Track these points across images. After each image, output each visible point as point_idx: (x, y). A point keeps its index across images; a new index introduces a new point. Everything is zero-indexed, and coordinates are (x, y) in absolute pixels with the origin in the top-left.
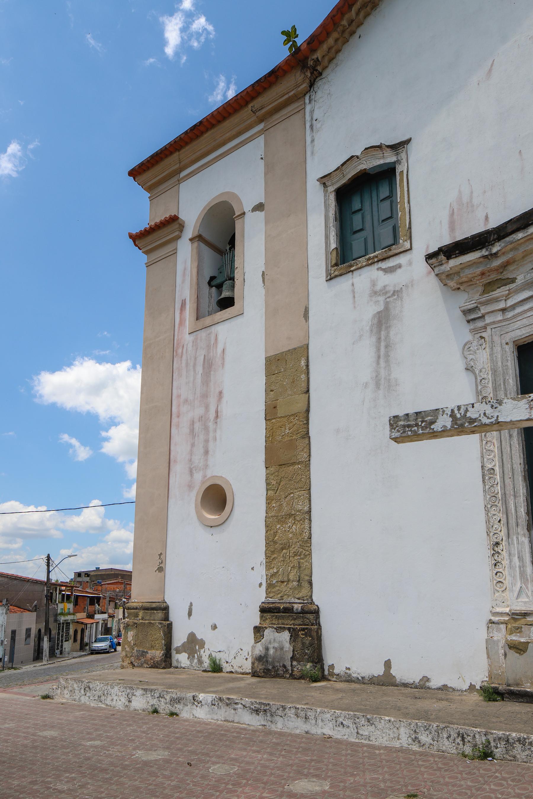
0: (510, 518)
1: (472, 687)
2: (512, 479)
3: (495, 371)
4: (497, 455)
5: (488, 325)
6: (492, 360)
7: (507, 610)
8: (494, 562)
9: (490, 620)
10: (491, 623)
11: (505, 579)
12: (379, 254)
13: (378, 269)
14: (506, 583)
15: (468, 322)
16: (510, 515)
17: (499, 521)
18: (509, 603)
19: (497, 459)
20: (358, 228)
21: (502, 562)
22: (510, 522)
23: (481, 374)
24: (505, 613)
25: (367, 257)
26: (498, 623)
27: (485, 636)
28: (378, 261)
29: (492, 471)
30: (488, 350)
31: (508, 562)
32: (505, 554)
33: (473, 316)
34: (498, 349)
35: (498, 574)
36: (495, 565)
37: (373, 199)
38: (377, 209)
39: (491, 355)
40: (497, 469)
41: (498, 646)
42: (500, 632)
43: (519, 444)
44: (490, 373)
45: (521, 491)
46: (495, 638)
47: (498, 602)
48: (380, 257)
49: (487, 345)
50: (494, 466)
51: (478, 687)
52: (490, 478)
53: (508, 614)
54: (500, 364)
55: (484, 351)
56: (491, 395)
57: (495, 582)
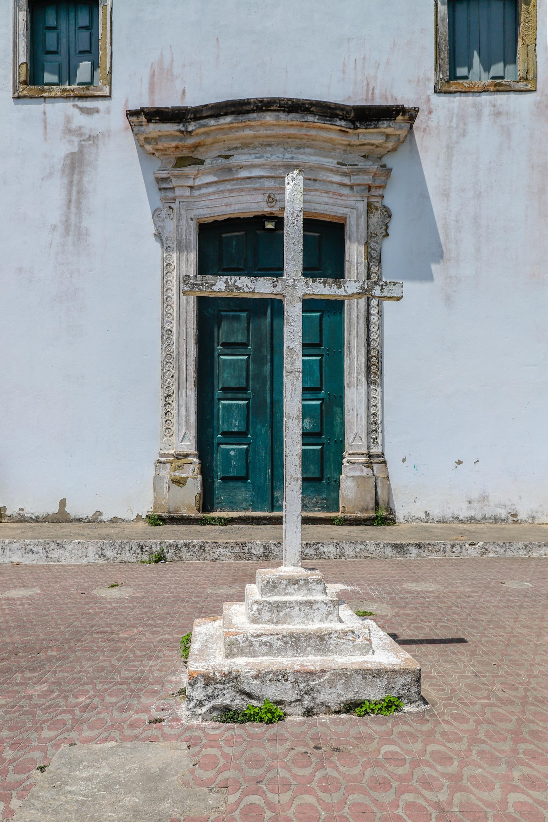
0: (181, 374)
1: (139, 518)
2: (185, 341)
3: (180, 242)
4: (175, 318)
5: (177, 197)
6: (178, 231)
7: (172, 452)
8: (165, 411)
9: (158, 460)
11: (173, 426)
12: (76, 89)
13: (74, 106)
14: (174, 429)
15: (160, 189)
16: (181, 371)
17: (172, 377)
18: (174, 446)
19: (174, 322)
20: (52, 49)
21: (172, 412)
22: (181, 377)
23: (167, 242)
24: (171, 454)
25: (62, 87)
26: (164, 463)
27: (153, 474)
28: (75, 97)
29: (170, 332)
30: (175, 220)
31: (176, 412)
32: (174, 404)
33: (164, 185)
34: (183, 222)
35: (168, 421)
36: (166, 414)
37: (71, 22)
38: (74, 36)
39: (178, 226)
40: (174, 331)
43: (194, 311)
44: (175, 243)
45: (192, 352)
46: (161, 475)
48: (77, 93)
49: (175, 216)
50: (172, 327)
51: (144, 516)
52: (168, 338)
53: (173, 455)
54: (184, 236)
55: (171, 221)
56: (175, 264)
57: (164, 428)
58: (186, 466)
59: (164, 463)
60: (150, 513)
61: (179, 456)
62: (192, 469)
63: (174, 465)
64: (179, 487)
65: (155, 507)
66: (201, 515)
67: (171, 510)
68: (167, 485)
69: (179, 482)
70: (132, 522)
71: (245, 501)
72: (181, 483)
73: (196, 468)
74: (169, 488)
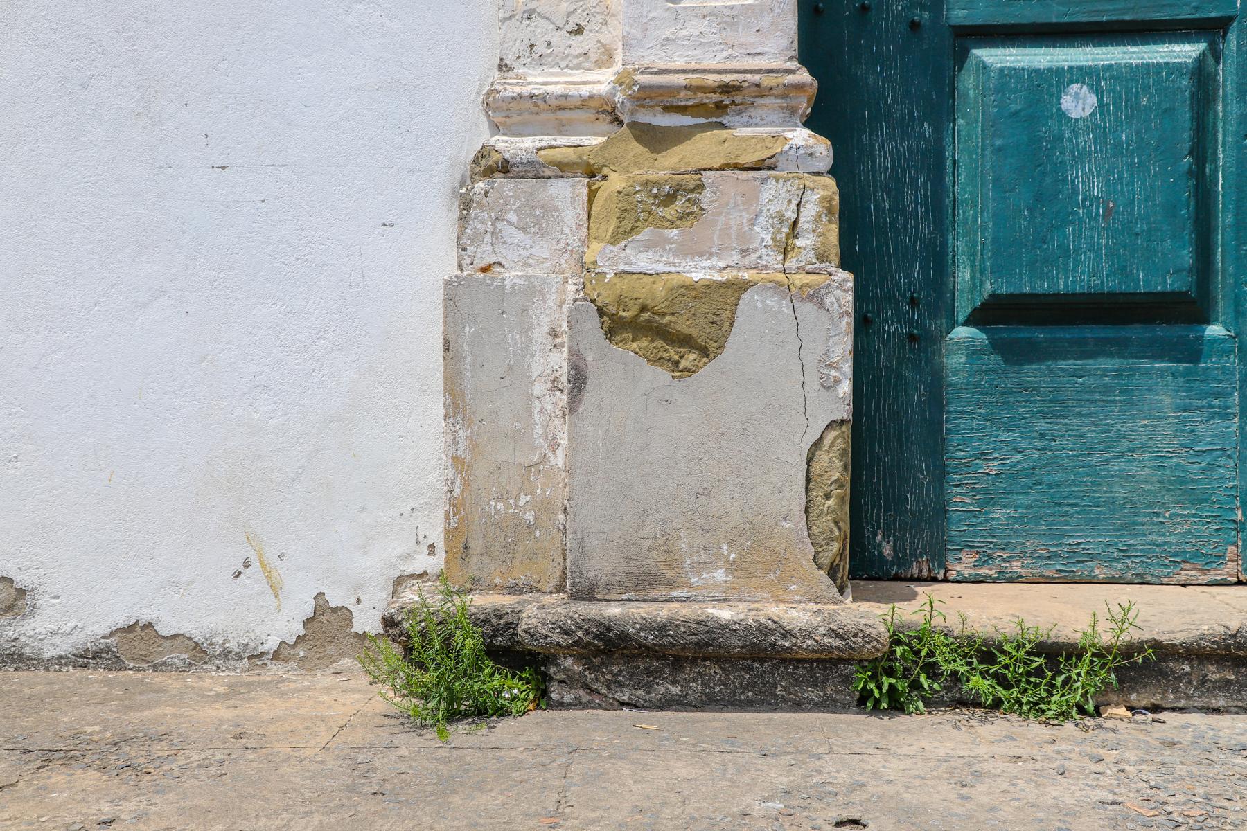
7: (601, 82)
9: (483, 153)
10: (489, 172)
18: (613, 34)
24: (584, 103)
26: (533, 170)
41: (526, 330)
42: (543, 233)
47: (540, 30)
58: (721, 192)
59: (533, 170)
60: (409, 596)
61: (669, 112)
62: (771, 216)
63: (615, 182)
64: (663, 375)
65: (459, 545)
66: (870, 616)
67: (600, 567)
68: (559, 362)
69: (669, 331)
70: (275, 670)
71: (1188, 492)
72: (685, 341)
73: (811, 210)
74: (578, 380)
